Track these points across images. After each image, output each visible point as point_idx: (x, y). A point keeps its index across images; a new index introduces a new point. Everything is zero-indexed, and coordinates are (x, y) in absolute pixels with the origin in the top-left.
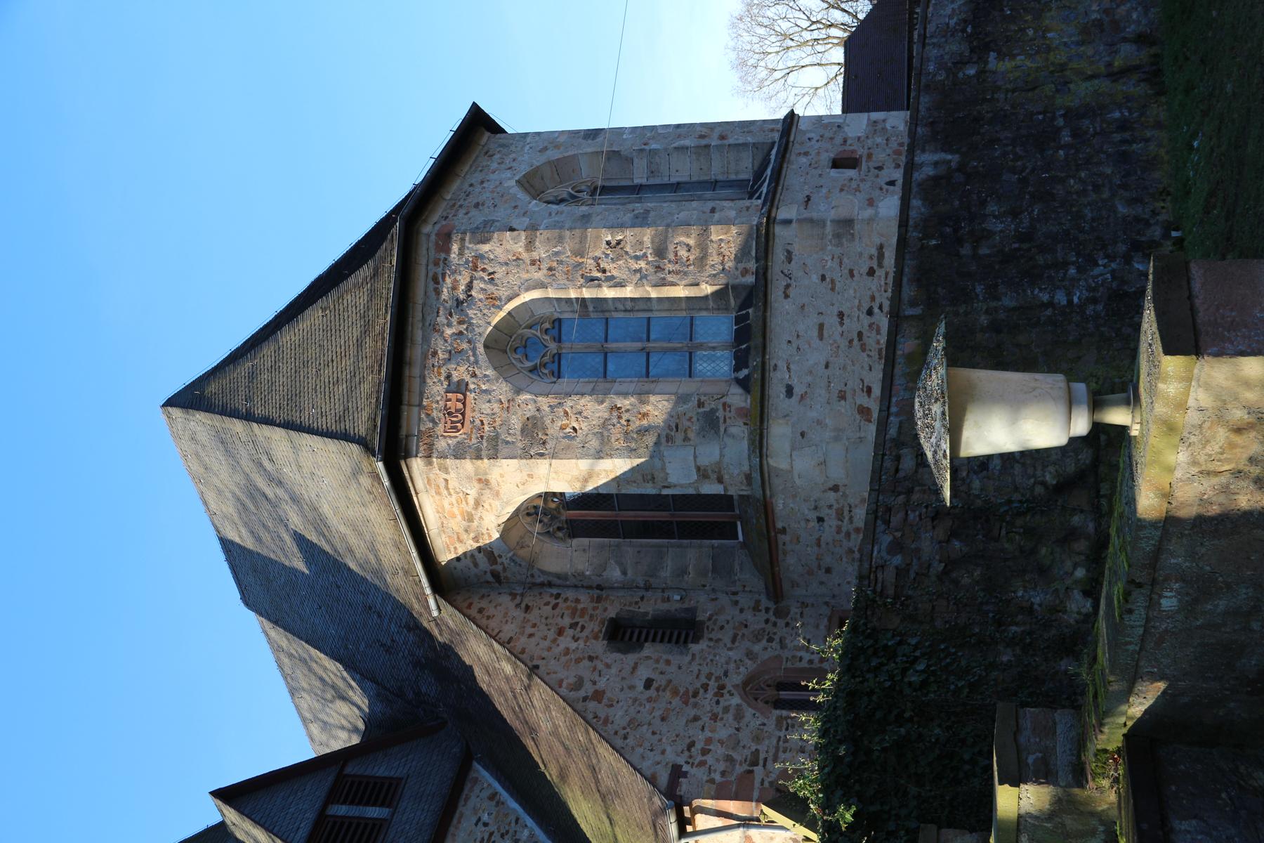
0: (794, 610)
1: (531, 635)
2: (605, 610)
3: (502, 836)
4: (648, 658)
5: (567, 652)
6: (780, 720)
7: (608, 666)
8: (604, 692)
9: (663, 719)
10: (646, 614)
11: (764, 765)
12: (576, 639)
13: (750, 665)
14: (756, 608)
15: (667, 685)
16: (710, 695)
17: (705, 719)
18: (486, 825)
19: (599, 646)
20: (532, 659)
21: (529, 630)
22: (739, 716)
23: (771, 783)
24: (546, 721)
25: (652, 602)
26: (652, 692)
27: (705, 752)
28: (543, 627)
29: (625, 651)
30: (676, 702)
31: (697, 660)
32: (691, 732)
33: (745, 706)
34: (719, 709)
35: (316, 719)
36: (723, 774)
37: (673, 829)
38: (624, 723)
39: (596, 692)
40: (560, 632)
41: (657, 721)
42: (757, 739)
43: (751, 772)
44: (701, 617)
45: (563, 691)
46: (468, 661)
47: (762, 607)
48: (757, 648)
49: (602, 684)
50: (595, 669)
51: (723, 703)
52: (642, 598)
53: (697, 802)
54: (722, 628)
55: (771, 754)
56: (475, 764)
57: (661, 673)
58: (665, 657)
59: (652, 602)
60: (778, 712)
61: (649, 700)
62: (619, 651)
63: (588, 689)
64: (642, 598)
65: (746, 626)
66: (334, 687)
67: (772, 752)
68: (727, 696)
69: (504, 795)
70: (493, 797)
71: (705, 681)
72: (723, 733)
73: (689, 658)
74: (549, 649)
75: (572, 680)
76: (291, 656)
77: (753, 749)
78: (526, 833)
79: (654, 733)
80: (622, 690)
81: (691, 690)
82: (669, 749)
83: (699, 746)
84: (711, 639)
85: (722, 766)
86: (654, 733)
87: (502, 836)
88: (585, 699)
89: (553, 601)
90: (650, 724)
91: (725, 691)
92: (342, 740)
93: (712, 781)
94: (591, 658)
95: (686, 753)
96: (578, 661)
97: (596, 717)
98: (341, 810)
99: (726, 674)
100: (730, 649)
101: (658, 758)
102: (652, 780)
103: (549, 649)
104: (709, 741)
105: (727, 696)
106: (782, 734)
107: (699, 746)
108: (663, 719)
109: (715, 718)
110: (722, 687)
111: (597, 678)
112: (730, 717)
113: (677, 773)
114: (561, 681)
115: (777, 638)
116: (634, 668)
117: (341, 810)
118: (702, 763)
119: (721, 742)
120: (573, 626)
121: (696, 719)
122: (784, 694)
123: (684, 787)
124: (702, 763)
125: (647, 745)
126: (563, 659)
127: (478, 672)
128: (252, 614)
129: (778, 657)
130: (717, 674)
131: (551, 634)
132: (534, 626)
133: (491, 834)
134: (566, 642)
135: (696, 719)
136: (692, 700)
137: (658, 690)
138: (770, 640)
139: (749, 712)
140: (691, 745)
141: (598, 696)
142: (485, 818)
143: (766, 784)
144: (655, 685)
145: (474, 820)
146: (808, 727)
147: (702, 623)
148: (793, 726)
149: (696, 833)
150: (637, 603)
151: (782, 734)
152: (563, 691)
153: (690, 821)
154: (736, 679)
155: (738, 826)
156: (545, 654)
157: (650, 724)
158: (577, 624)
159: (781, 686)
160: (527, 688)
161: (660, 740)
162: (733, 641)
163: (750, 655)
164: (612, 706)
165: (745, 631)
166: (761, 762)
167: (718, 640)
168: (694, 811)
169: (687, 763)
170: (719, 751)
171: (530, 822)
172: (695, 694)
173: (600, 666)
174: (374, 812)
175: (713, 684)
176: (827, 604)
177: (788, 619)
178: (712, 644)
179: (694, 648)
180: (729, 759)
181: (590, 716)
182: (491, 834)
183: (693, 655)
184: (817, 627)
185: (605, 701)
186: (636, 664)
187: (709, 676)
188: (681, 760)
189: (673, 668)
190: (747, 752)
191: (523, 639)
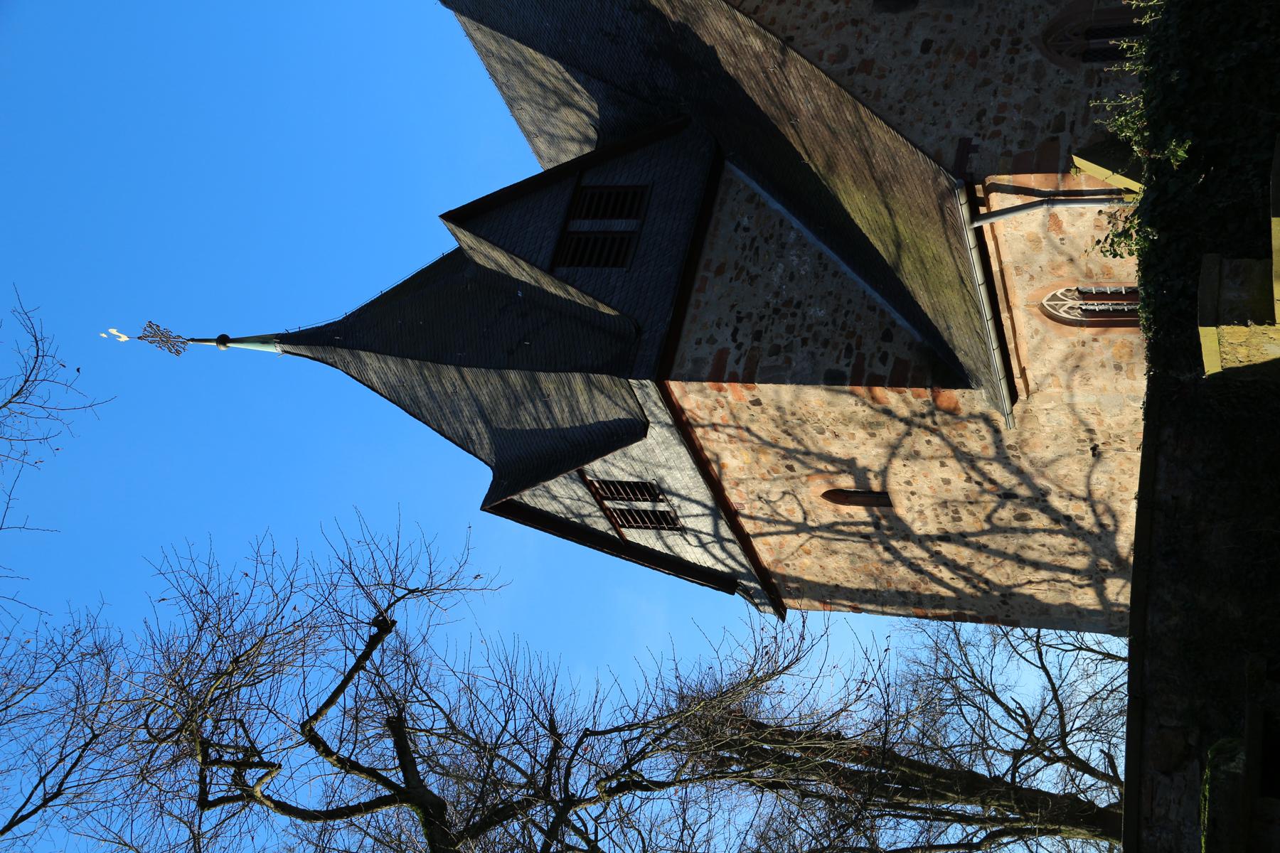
3: (766, 241)
7: (876, 30)
8: (873, 61)
9: (946, 87)
11: (1072, 130)
18: (746, 229)
20: (784, 29)
22: (1039, 74)
24: (805, 98)
26: (931, 56)
27: (998, 121)
35: (542, 132)
36: (1021, 144)
37: (964, 212)
43: (1055, 139)
45: (825, 63)
46: (708, 41)
49: (870, 52)
50: (860, 34)
53: (991, 179)
56: (727, 163)
57: (942, 32)
60: (1087, 66)
61: (929, 65)
63: (854, 59)
66: (556, 92)
69: (764, 195)
70: (752, 198)
74: (804, 16)
75: (833, 51)
76: (502, 61)
77: (1058, 111)
78: (793, 235)
79: (936, 104)
80: (895, 56)
82: (955, 121)
83: (991, 114)
85: (1019, 135)
86: (936, 104)
87: (766, 241)
88: (851, 71)
90: (930, 94)
91: (1021, 46)
92: (572, 151)
93: (1008, 153)
94: (855, 23)
95: (976, 124)
96: (840, 27)
98: (584, 225)
99: (1021, 26)
102: (937, 158)
104: (1003, 107)
106: (1093, 91)
107: (991, 114)
108: (946, 87)
109: (1009, 79)
110: (1016, 42)
113: (965, 147)
114: (822, 52)
116: (909, 29)
117: (584, 225)
118: (996, 134)
121: (986, 82)
122: (1095, 43)
123: (975, 162)
124: (996, 134)
127: (722, 53)
128: (449, 13)
133: (754, 240)
135: (986, 82)
136: (981, 61)
137: (938, 52)
141: (866, 66)
142: (745, 222)
144: (934, 47)
145: (733, 226)
146: (1133, 59)
148: (1107, 80)
149: (992, 214)
152: (825, 63)
153: (985, 202)
155: (1041, 203)
159: (1091, 33)
160: (782, 65)
161: (944, 112)
164: (882, 77)
166: (1068, 126)
168: (989, 189)
169: (978, 135)
171: (796, 223)
172: (985, 53)
174: (620, 225)
175: (1005, 38)
180: (1028, 127)
182: (754, 240)
183: (980, 6)
185: (875, 71)
187: (1000, 30)
188: (969, 133)
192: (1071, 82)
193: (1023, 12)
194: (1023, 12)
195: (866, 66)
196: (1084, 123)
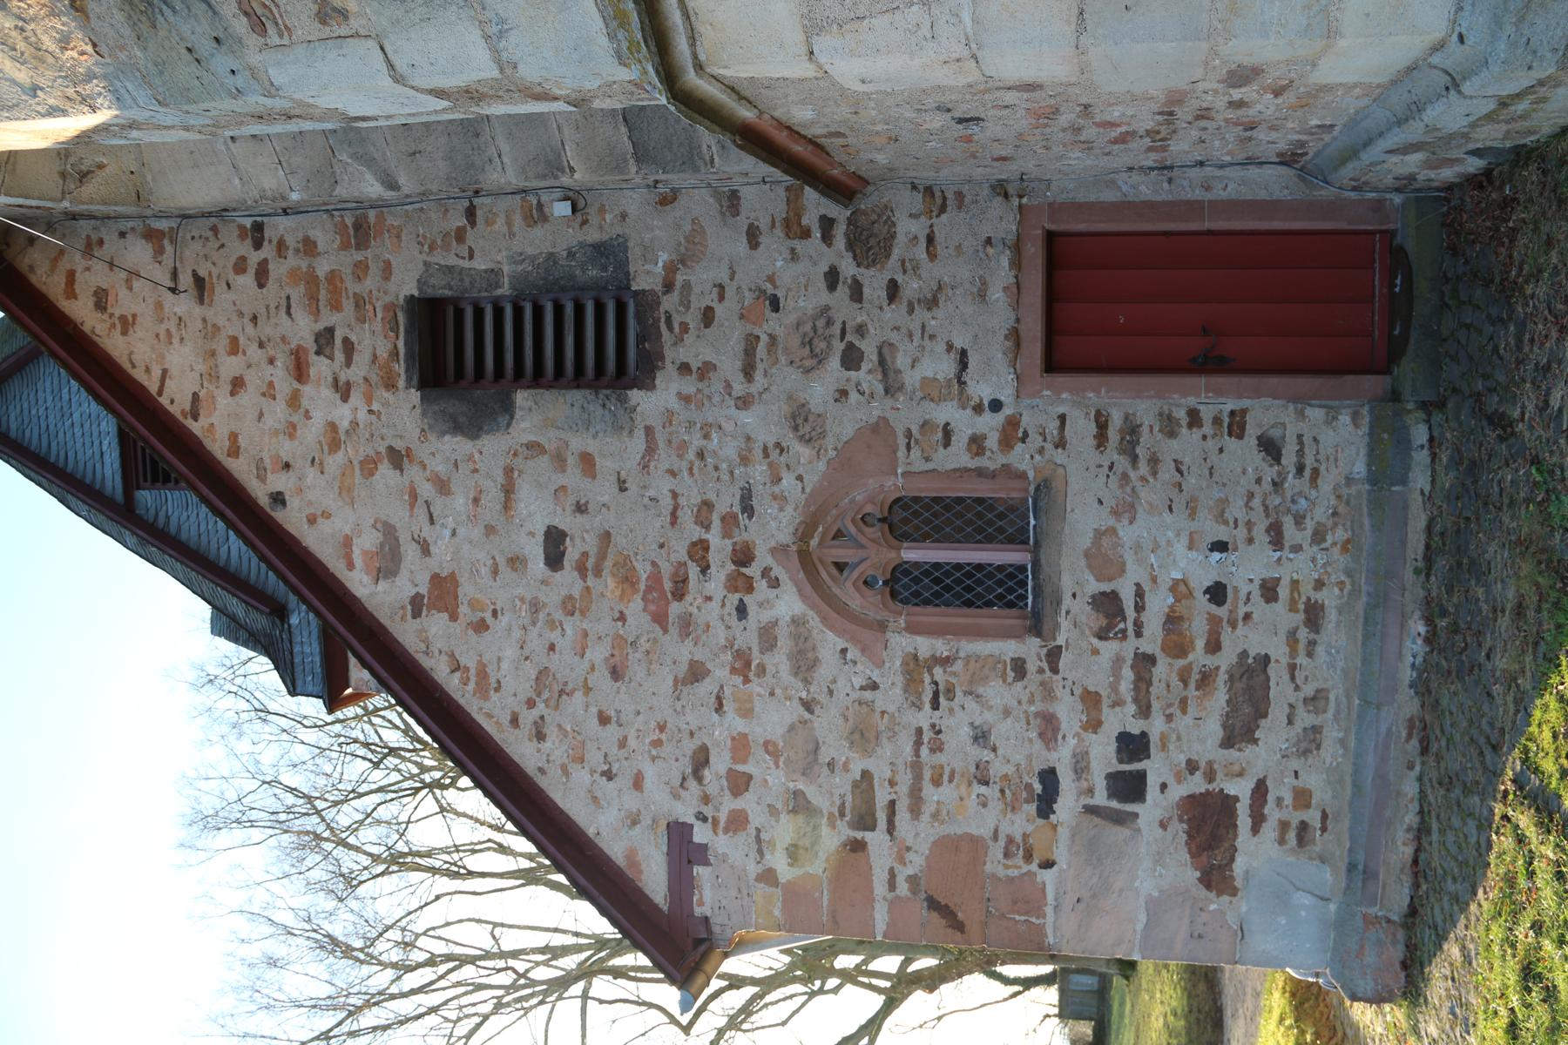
0: (907, 227)
1: (237, 384)
2: (387, 270)
4: (535, 448)
5: (334, 439)
6: (914, 667)
7: (443, 487)
10: (494, 274)
11: (891, 828)
12: (343, 391)
13: (808, 467)
14: (794, 228)
15: (602, 556)
16: (716, 584)
17: (720, 672)
19: (404, 410)
21: (230, 366)
22: (804, 664)
23: (913, 880)
25: (500, 225)
26: (567, 579)
27: (739, 783)
28: (253, 352)
29: (471, 427)
30: (634, 607)
31: (665, 458)
32: (693, 719)
33: (814, 621)
34: (748, 637)
38: (526, 689)
39: (436, 579)
40: (300, 372)
41: (601, 679)
42: (862, 736)
43: (858, 846)
44: (646, 277)
47: (810, 219)
48: (818, 391)
49: (443, 557)
51: (756, 616)
52: (471, 213)
54: (708, 316)
55: (903, 789)
57: (581, 508)
58: (579, 442)
59: (500, 225)
62: (457, 428)
63: (413, 578)
64: (471, 213)
65: (775, 305)
67: (905, 779)
68: (761, 585)
71: (697, 533)
72: (774, 719)
73: (638, 444)
75: (368, 541)
79: (604, 720)
80: (495, 572)
81: (666, 569)
82: (650, 772)
83: (720, 763)
84: (685, 368)
88: (416, 606)
89: (255, 257)
90: (588, 690)
91: (753, 571)
93: (768, 877)
94: (397, 458)
96: (369, 466)
97: (456, 667)
100: (744, 403)
101: (631, 801)
103: (291, 430)
105: (761, 585)
108: (616, 674)
110: (743, 557)
111: (427, 532)
112: (779, 662)
114: (347, 543)
115: (868, 347)
116: (508, 491)
119: (769, 747)
120: (324, 339)
121: (696, 673)
124: (738, 821)
125: (594, 757)
126: (335, 462)
129: (881, 428)
130: (722, 507)
131: (280, 375)
132: (234, 347)
134: (321, 403)
135: (696, 673)
136: (675, 608)
137: (581, 569)
138: (852, 359)
139: (829, 643)
140: (701, 760)
143: (903, 888)
144: (572, 554)
147: (647, 302)
150: (460, 236)
151: (925, 718)
154: (774, 527)
156: (287, 449)
157: (588, 690)
158: (330, 331)
161: (623, 744)
162: (748, 372)
163: (801, 419)
164: (481, 627)
165: (774, 324)
166: (881, 817)
167: (706, 370)
170: (773, 779)
173: (426, 490)
176: (1001, 189)
177: (891, 269)
178: (689, 386)
179: (649, 403)
181: (439, 670)
184: (982, 295)
185: (463, 609)
186: (508, 471)
188: (686, 813)
189: (601, 491)
190: (842, 784)
191: (223, 401)
192: (874, 686)
193: (745, 460)
194: (745, 460)
195: (442, 593)
196: (915, 811)
